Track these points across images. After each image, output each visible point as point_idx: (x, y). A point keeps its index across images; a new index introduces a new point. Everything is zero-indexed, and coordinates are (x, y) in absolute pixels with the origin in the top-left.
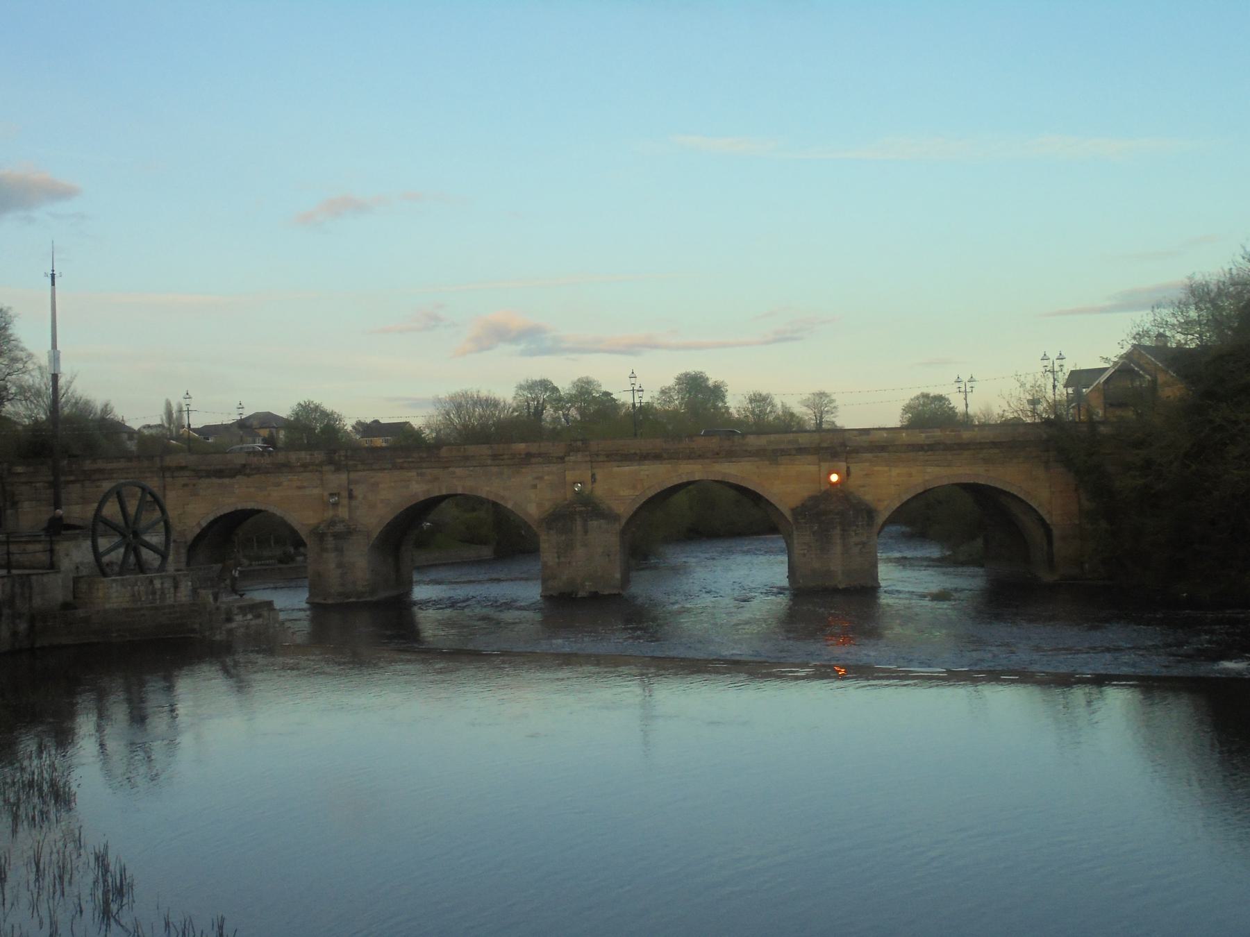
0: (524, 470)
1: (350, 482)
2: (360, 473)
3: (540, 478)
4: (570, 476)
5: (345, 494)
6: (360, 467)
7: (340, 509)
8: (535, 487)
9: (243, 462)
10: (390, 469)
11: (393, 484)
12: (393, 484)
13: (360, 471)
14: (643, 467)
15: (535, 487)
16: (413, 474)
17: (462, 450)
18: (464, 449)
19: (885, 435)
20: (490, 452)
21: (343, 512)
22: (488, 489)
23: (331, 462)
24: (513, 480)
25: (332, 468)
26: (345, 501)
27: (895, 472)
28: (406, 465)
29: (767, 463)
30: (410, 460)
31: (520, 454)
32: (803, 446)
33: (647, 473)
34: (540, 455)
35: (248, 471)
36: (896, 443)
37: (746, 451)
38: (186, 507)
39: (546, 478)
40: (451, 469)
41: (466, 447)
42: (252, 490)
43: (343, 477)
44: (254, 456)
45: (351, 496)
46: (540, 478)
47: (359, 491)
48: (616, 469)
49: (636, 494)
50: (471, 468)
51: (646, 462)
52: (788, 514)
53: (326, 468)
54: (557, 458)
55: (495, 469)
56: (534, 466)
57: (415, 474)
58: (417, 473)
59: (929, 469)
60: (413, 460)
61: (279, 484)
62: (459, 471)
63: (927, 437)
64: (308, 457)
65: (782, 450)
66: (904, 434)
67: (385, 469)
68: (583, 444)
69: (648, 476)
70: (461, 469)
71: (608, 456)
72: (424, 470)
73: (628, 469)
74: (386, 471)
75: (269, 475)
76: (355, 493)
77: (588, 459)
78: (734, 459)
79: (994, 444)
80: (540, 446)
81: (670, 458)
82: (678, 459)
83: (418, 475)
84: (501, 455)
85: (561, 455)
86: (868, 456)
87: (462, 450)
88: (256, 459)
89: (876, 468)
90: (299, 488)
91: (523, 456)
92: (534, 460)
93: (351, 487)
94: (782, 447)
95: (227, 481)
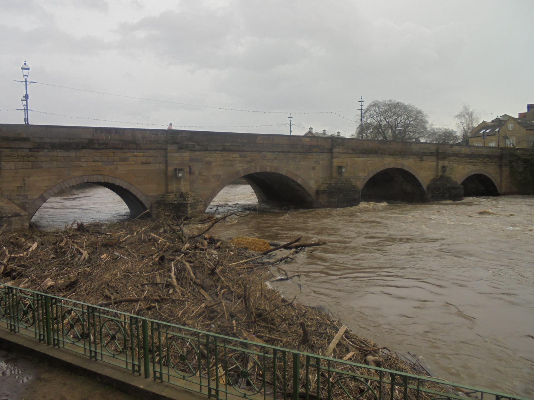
0: (309, 156)
1: (191, 160)
2: (197, 153)
4: (336, 162)
6: (197, 147)
7: (182, 183)
8: (314, 168)
10: (221, 151)
14: (369, 158)
15: (314, 168)
16: (236, 155)
19: (458, 148)
21: (184, 187)
22: (286, 169)
24: (302, 163)
25: (176, 147)
26: (187, 176)
27: (461, 167)
29: (419, 159)
33: (371, 162)
36: (461, 153)
38: (26, 179)
39: (321, 162)
40: (263, 153)
42: (100, 164)
43: (186, 155)
45: (191, 173)
47: (196, 168)
48: (356, 159)
50: (277, 153)
52: (425, 187)
53: (170, 147)
55: (291, 155)
56: (314, 154)
57: (238, 155)
59: (471, 167)
61: (125, 160)
62: (269, 155)
64: (153, 136)
66: (463, 149)
69: (371, 164)
70: (270, 153)
71: (353, 150)
73: (360, 159)
74: (218, 152)
75: (115, 150)
79: (488, 156)
81: (382, 154)
82: (385, 154)
83: (241, 156)
86: (452, 158)
88: (103, 134)
90: (143, 163)
92: (315, 150)
94: (425, 151)
95: (73, 154)
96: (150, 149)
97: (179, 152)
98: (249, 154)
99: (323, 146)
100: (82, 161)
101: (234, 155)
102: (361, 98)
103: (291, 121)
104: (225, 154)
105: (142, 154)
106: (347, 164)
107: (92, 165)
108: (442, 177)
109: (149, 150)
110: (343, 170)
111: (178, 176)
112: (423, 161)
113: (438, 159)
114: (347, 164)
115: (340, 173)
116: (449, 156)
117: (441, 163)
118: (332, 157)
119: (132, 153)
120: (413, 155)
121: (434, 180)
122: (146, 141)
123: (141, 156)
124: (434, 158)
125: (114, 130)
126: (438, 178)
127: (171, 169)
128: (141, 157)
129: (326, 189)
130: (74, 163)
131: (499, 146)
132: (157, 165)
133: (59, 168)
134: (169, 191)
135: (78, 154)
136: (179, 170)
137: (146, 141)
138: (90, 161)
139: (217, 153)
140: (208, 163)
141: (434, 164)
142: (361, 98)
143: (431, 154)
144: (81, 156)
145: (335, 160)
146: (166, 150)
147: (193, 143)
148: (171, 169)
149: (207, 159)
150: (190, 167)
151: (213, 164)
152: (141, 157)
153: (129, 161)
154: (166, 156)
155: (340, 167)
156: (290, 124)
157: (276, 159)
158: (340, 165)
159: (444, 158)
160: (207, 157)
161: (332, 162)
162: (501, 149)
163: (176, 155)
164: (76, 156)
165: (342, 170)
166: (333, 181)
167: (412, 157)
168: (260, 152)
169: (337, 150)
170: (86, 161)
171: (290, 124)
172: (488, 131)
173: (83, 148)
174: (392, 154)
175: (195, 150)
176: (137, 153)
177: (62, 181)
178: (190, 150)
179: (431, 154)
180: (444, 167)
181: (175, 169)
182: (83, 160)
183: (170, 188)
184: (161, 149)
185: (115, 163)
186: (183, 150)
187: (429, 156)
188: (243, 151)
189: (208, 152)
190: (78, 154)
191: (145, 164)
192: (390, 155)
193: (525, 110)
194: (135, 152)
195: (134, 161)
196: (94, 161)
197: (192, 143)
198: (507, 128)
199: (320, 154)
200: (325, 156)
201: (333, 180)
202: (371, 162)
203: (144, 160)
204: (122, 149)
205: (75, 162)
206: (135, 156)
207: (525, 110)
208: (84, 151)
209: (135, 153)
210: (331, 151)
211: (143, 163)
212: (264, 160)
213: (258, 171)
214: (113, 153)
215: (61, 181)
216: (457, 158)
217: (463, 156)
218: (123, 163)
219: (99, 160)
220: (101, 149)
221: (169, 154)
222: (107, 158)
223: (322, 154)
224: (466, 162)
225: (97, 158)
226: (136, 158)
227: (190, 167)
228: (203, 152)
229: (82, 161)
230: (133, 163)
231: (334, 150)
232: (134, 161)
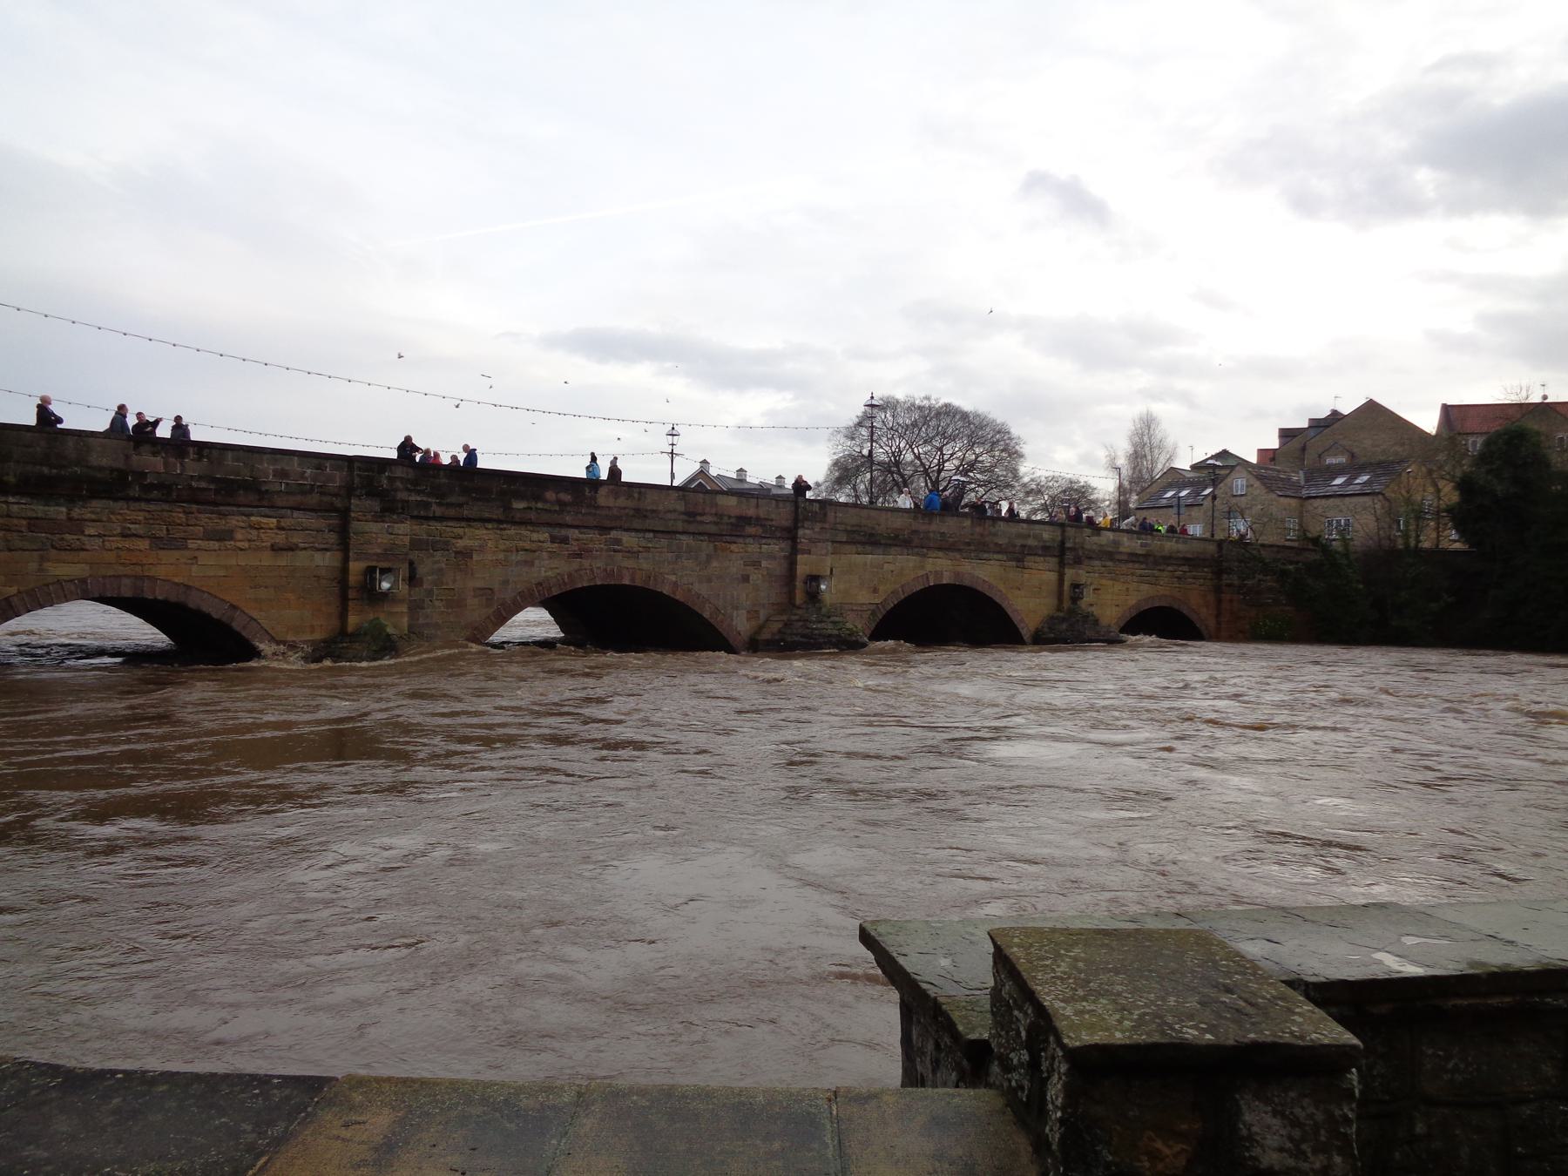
0: (733, 547)
1: (416, 544)
2: (436, 526)
3: (756, 564)
5: (404, 570)
8: (746, 579)
9: (120, 464)
10: (499, 521)
11: (501, 556)
12: (501, 556)
13: (435, 518)
15: (746, 579)
16: (543, 535)
17: (636, 495)
18: (640, 493)
20: (680, 507)
22: (673, 578)
23: (372, 491)
25: (376, 505)
26: (403, 588)
28: (532, 516)
29: (1014, 563)
30: (540, 505)
31: (730, 517)
32: (1048, 544)
33: (891, 567)
34: (758, 521)
35: (135, 491)
36: (1121, 549)
37: (996, 544)
39: (764, 564)
40: (614, 534)
41: (643, 490)
42: (144, 544)
43: (405, 530)
44: (155, 454)
45: (413, 579)
46: (756, 564)
49: (877, 601)
50: (651, 535)
51: (893, 550)
54: (784, 529)
56: (747, 540)
58: (551, 536)
59: (1145, 587)
60: (547, 506)
61: (224, 536)
62: (629, 540)
63: (1142, 545)
64: (309, 471)
65: (1030, 547)
67: (489, 520)
68: (820, 508)
72: (564, 532)
74: (490, 526)
75: (195, 507)
76: (422, 570)
77: (828, 536)
78: (986, 556)
80: (757, 506)
82: (929, 548)
83: (553, 539)
84: (701, 515)
85: (787, 523)
87: (636, 495)
89: (1104, 582)
90: (275, 548)
91: (733, 520)
92: (750, 530)
93: (414, 555)
95: (59, 511)
96: (298, 509)
97: (383, 521)
98: (573, 533)
99: (772, 520)
100: (87, 533)
101: (535, 536)
102: (872, 398)
103: (673, 445)
104: (512, 531)
105: (274, 520)
106: (832, 570)
107: (118, 548)
108: (1071, 612)
109: (296, 514)
110: (823, 587)
111: (380, 588)
112: (1024, 568)
113: (1062, 564)
114: (832, 570)
115: (813, 596)
116: (1090, 558)
117: (1070, 574)
118: (794, 551)
119: (244, 518)
120: (999, 553)
121: (1051, 619)
122: (287, 484)
123: (272, 526)
124: (1053, 562)
125: (191, 450)
126: (1061, 614)
127: (356, 567)
128: (271, 529)
129: (777, 637)
130: (62, 539)
131: (1213, 535)
132: (318, 556)
133: (10, 550)
134: (350, 629)
135: (76, 513)
136: (384, 571)
137: (287, 484)
138: (114, 536)
139: (487, 529)
140: (466, 554)
141: (1052, 577)
142: (872, 398)
143: (1046, 550)
144: (86, 520)
145: (799, 557)
146: (347, 510)
147: (425, 499)
148: (356, 567)
149: (461, 543)
150: (411, 563)
151: (475, 557)
152: (271, 529)
153: (235, 541)
154: (343, 532)
155: (814, 579)
156: (672, 453)
157: (647, 549)
158: (815, 573)
159: (1078, 562)
160: (461, 538)
161: (792, 564)
162: (1220, 543)
163: (374, 527)
164: (70, 519)
165: (818, 586)
166: (796, 615)
167: (996, 556)
168: (604, 530)
169: (807, 532)
170: (99, 536)
171: (672, 453)
172: (1184, 493)
173: (94, 495)
174: (947, 546)
175: (427, 518)
176: (259, 518)
177: (19, 592)
178: (412, 517)
179: (1046, 550)
180: (1075, 586)
181: (371, 571)
182: (92, 532)
183: (353, 620)
184: (334, 509)
185: (191, 544)
186: (395, 517)
187: (1040, 556)
188: (561, 525)
189: (463, 524)
190: (76, 513)
191: (282, 549)
192: (940, 549)
193: (1273, 443)
194: (252, 515)
195: (249, 541)
196: (124, 536)
197: (419, 499)
198: (1231, 488)
199: (764, 541)
200: (777, 548)
201: (795, 611)
202: (891, 567)
203: (280, 538)
204: (216, 504)
205: (67, 536)
206: (252, 527)
207: (1273, 443)
208: (97, 504)
209: (252, 518)
210: (790, 534)
211: (275, 548)
212: (615, 551)
213: (599, 583)
214: (184, 512)
215: (15, 592)
216: (1109, 563)
217: (1125, 557)
218: (216, 545)
219: (141, 532)
220: (148, 501)
221: (355, 525)
222: (168, 530)
223: (769, 541)
224: (1133, 574)
225: (137, 526)
226: (254, 532)
227: (411, 563)
228: (450, 524)
229: (87, 533)
230: (246, 545)
231: (801, 532)
232: (249, 541)
